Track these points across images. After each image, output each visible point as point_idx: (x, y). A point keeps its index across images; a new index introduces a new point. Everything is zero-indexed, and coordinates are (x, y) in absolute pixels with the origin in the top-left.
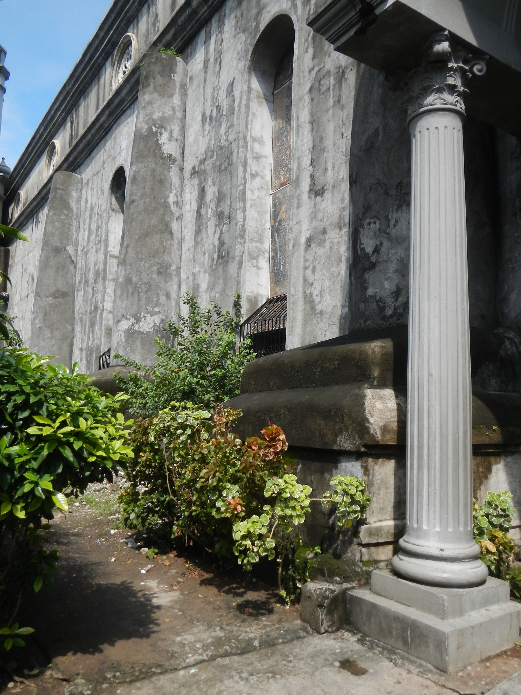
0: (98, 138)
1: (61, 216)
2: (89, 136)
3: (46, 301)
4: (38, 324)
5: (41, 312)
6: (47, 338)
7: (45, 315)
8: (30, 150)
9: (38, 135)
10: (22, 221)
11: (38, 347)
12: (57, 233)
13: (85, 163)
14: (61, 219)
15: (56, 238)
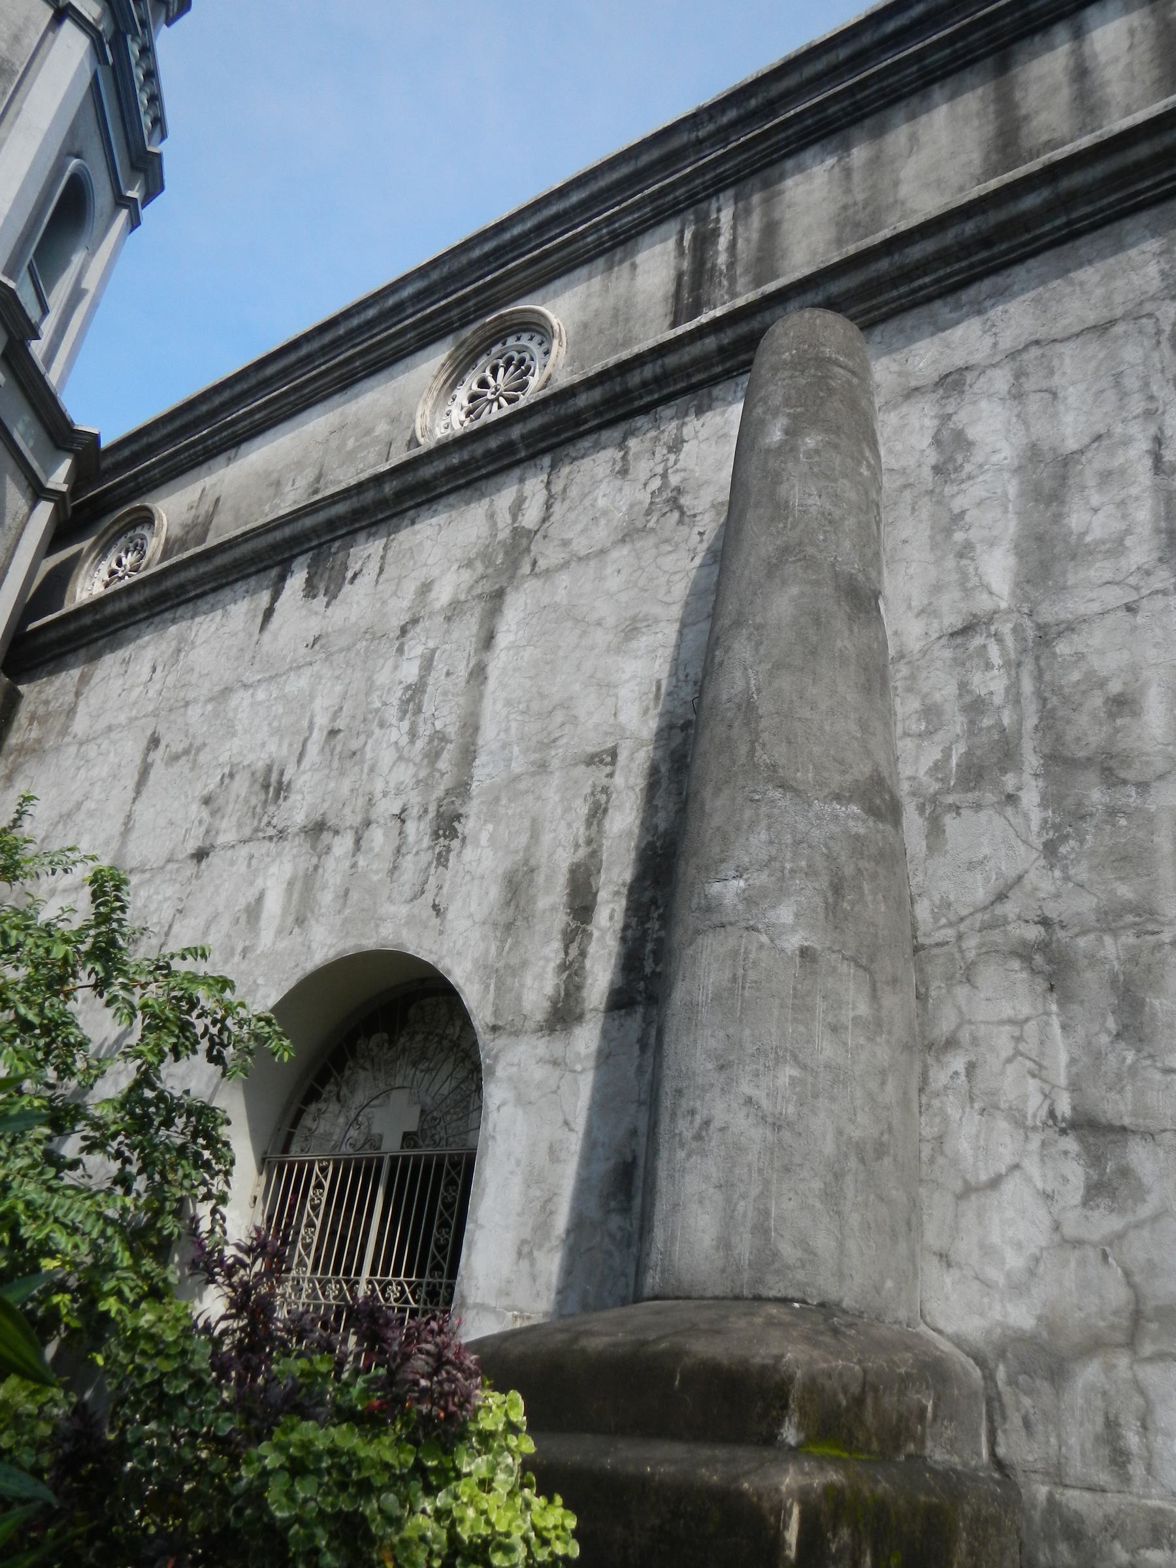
0: (1110, 206)
1: (859, 463)
2: (1030, 202)
3: (835, 818)
4: (793, 929)
5: (811, 872)
6: (856, 1020)
7: (837, 888)
8: (270, 371)
9: (371, 313)
10: (182, 588)
11: (804, 1067)
12: (850, 523)
13: (909, 320)
14: (861, 474)
15: (847, 544)
